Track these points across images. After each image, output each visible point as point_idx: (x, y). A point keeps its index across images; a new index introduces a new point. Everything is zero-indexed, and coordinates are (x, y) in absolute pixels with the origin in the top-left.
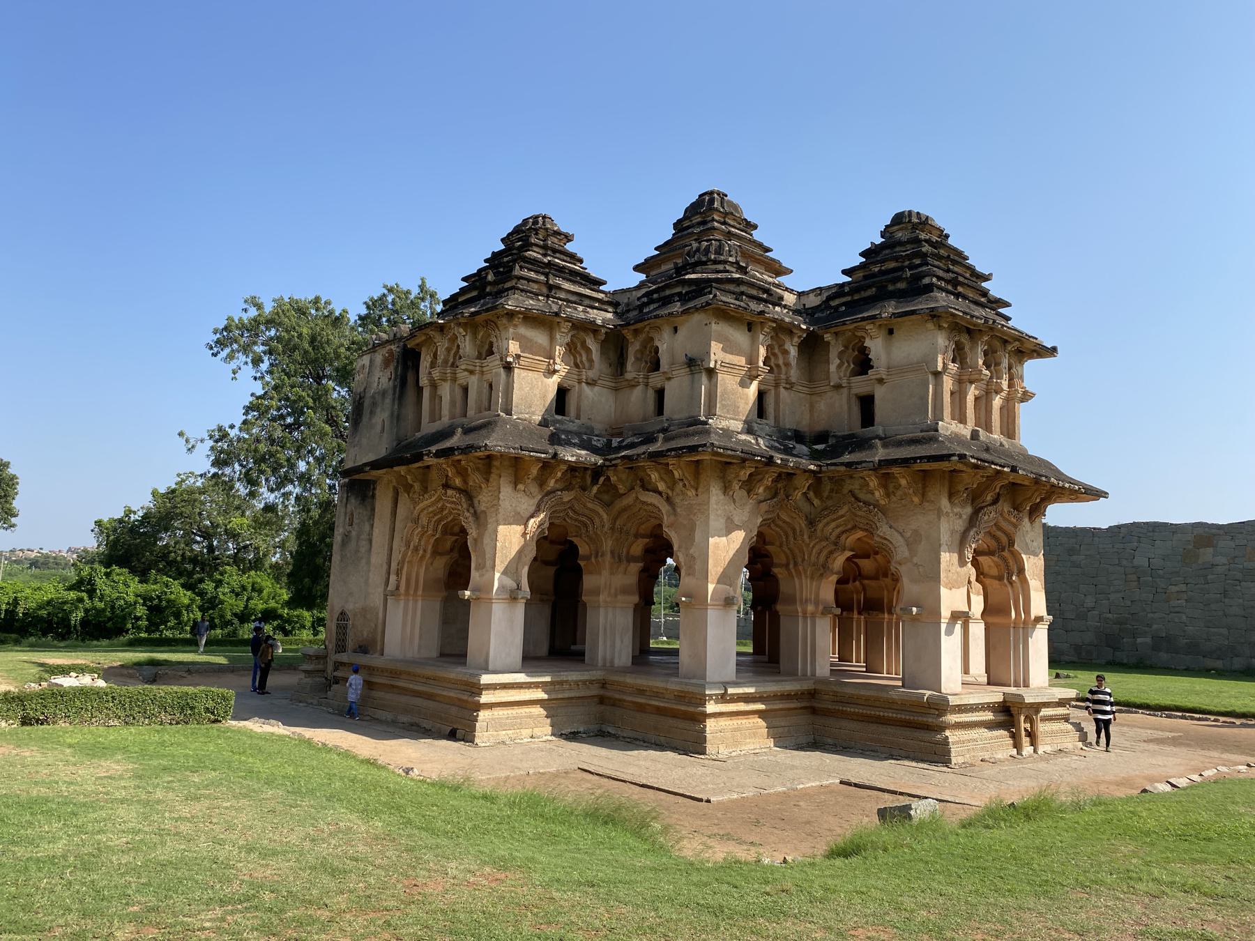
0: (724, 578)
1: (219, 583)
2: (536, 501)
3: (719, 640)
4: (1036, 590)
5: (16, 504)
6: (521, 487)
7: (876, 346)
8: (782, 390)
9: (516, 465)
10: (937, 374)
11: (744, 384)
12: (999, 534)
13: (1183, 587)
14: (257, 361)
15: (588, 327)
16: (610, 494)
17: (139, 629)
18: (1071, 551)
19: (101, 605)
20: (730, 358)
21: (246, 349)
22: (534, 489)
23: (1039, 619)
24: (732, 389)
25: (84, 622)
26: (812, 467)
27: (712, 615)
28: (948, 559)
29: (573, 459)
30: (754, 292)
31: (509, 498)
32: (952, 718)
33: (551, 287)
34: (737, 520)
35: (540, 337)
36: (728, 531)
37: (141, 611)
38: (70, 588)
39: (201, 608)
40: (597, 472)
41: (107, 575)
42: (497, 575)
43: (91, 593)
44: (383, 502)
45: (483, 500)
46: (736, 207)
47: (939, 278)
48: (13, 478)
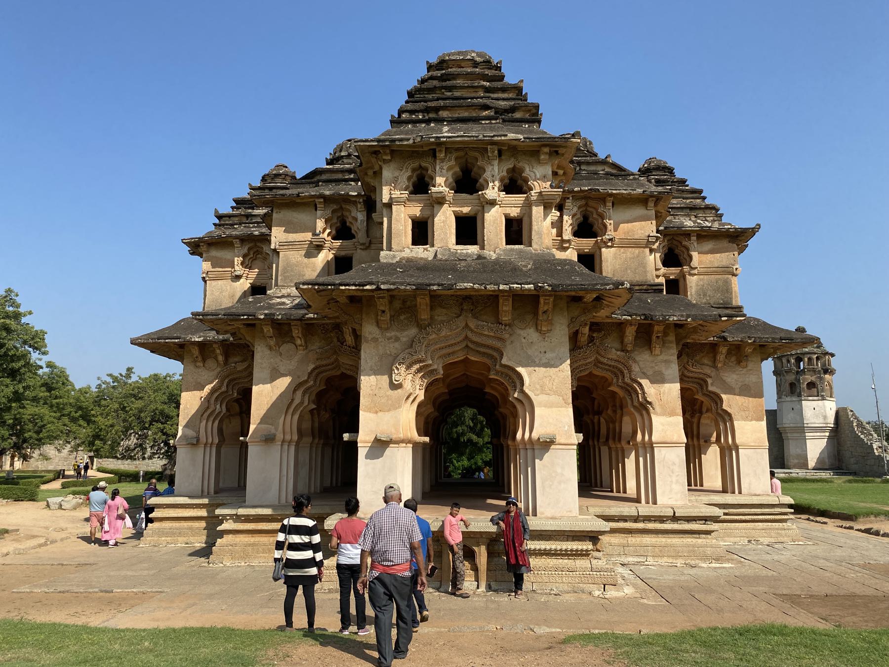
2: (215, 372)
4: (550, 405)
6: (198, 364)
8: (359, 251)
10: (389, 206)
11: (308, 255)
12: (482, 350)
22: (210, 363)
26: (311, 315)
29: (201, 339)
30: (340, 176)
33: (248, 216)
34: (282, 369)
36: (272, 379)
42: (180, 428)
47: (412, 112)
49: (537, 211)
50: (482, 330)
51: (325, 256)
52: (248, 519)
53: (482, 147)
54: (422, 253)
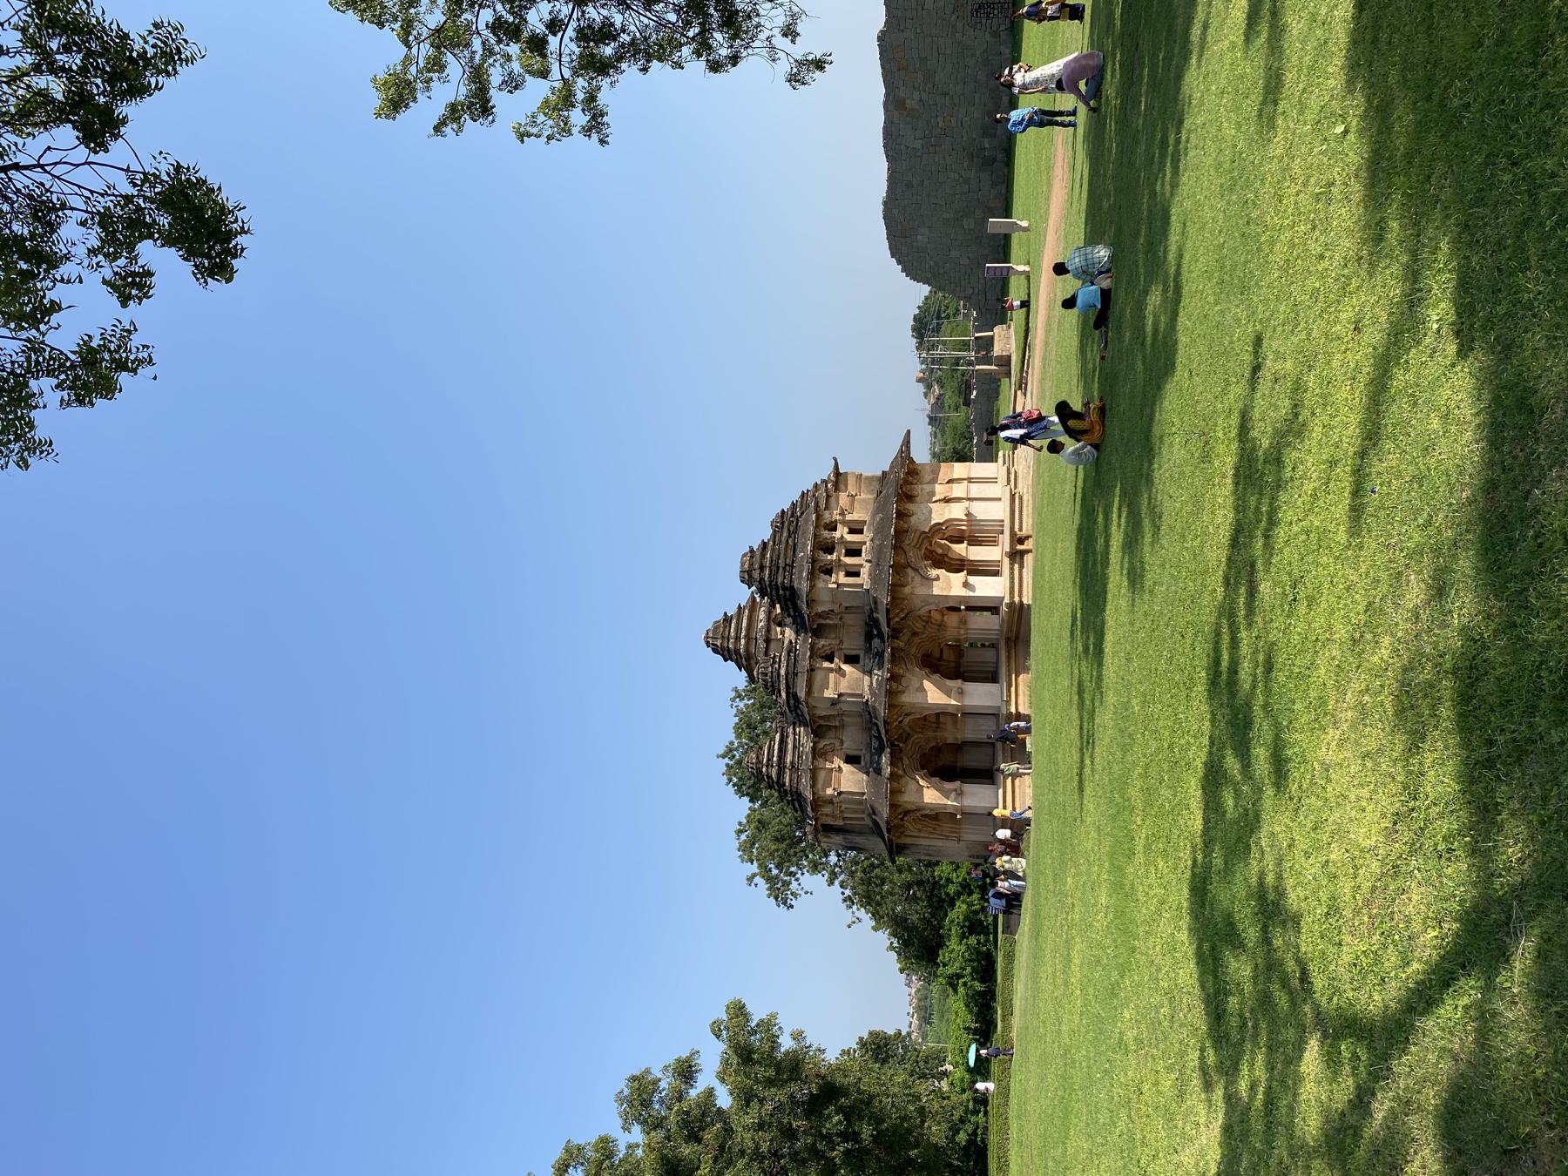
0: (948, 694)
1: (949, 881)
3: (980, 695)
5: (891, 1032)
7: (820, 609)
9: (895, 792)
11: (844, 675)
13: (940, 119)
14: (792, 874)
15: (814, 748)
16: (905, 738)
17: (987, 941)
18: (909, 185)
19: (969, 969)
20: (831, 685)
21: (787, 884)
22: (903, 781)
23: (968, 514)
24: (847, 682)
25: (982, 981)
27: (967, 702)
28: (937, 589)
31: (908, 798)
32: (1017, 599)
35: (822, 775)
37: (973, 940)
38: (956, 991)
39: (971, 893)
40: (893, 745)
41: (945, 965)
43: (959, 976)
44: (908, 841)
45: (909, 807)
46: (716, 628)
48: (871, 1033)
49: (848, 517)
50: (909, 540)
51: (845, 667)
52: (1009, 696)
53: (815, 535)
54: (865, 572)
